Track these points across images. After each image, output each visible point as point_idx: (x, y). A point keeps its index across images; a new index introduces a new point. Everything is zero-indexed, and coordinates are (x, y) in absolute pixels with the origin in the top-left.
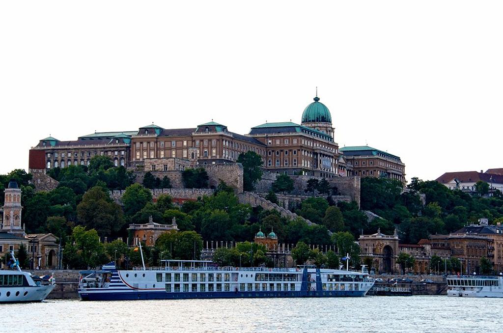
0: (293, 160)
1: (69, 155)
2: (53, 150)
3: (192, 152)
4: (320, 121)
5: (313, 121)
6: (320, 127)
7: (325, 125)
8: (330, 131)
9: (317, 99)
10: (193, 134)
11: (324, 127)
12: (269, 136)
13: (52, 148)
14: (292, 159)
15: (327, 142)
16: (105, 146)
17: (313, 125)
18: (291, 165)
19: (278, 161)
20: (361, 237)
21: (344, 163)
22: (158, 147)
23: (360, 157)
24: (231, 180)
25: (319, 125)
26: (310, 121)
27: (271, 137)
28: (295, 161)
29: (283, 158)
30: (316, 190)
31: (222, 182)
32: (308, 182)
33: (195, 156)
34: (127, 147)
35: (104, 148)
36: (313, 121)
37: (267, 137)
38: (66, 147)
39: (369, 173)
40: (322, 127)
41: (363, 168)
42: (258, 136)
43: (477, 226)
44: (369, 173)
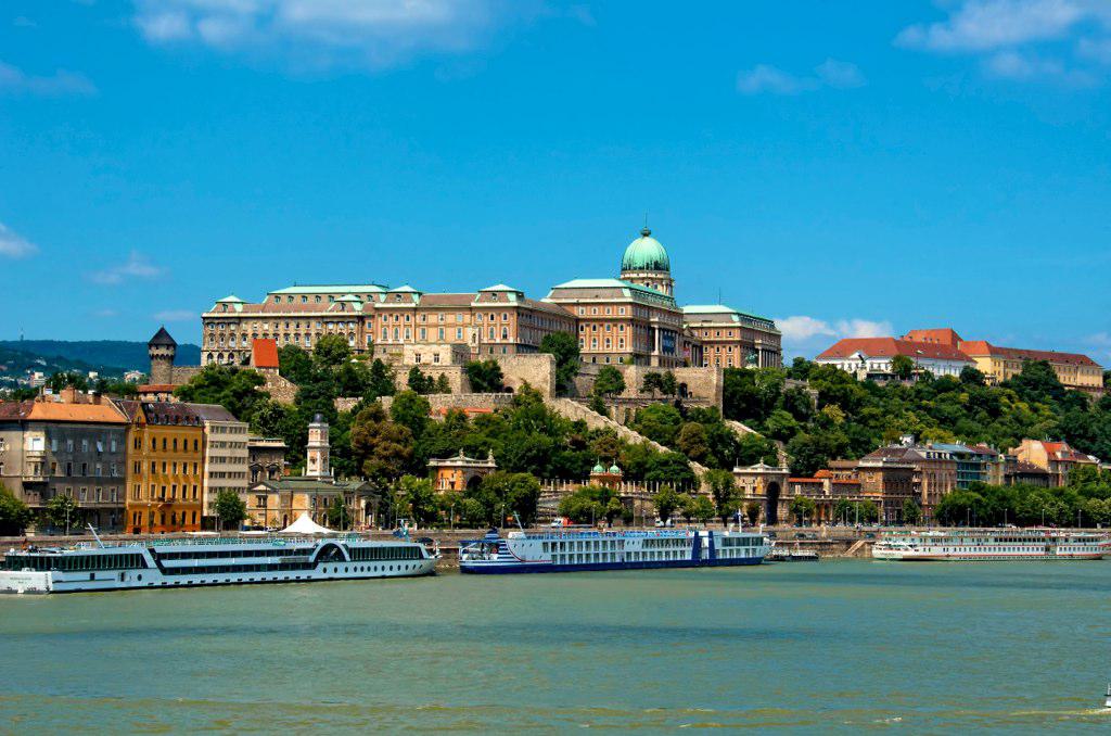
1: (266, 327)
2: (240, 318)
5: (640, 268)
10: (473, 304)
13: (236, 315)
16: (324, 314)
17: (641, 275)
18: (615, 348)
19: (595, 340)
20: (736, 470)
23: (712, 325)
24: (537, 379)
25: (650, 275)
26: (635, 269)
28: (622, 341)
30: (657, 389)
31: (525, 383)
32: (646, 377)
33: (477, 338)
34: (358, 317)
35: (323, 317)
37: (578, 304)
38: (261, 314)
43: (898, 446)
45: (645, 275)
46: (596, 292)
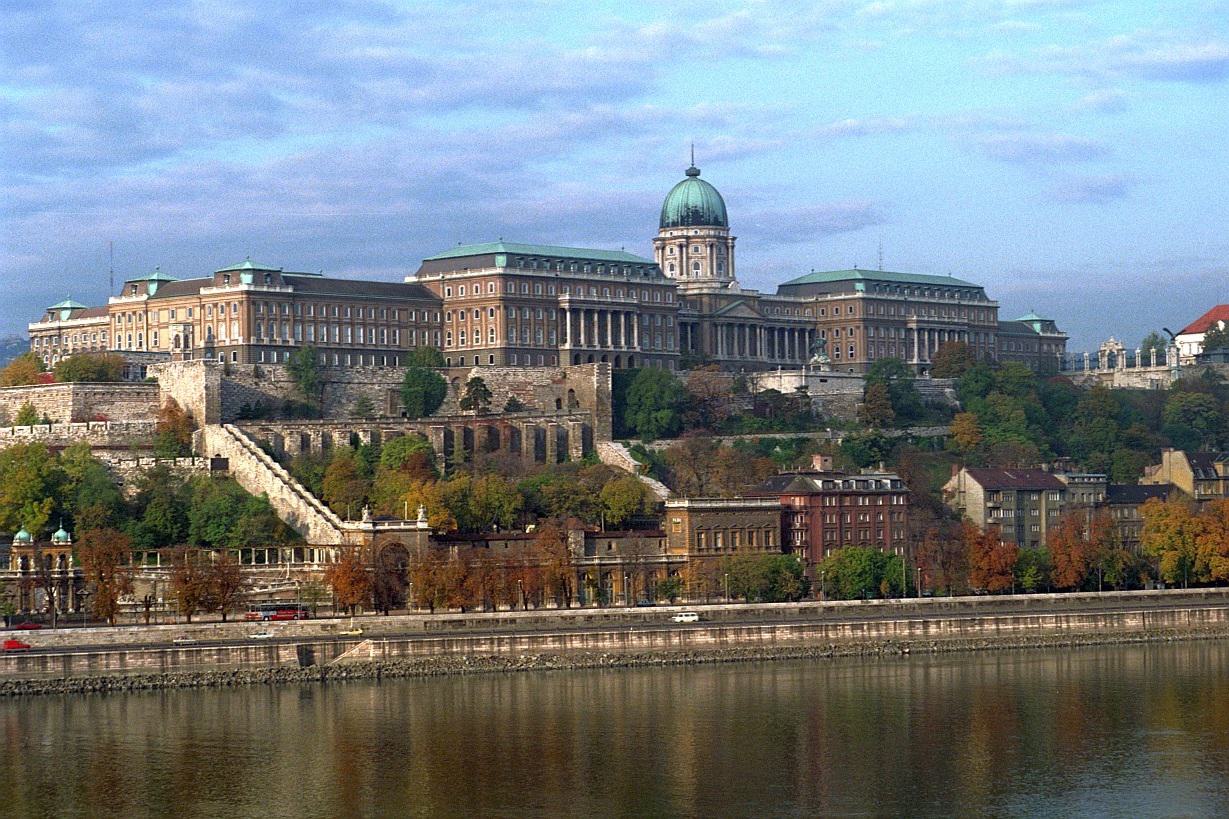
0: (489, 330)
3: (175, 333)
4: (688, 225)
6: (688, 238)
7: (700, 233)
8: (711, 246)
9: (693, 173)
11: (699, 237)
12: (448, 277)
14: (486, 329)
15: (624, 280)
17: (675, 233)
21: (755, 315)
22: (150, 322)
25: (685, 233)
27: (450, 280)
29: (472, 328)
36: (675, 224)
37: (443, 281)
39: (846, 334)
40: (694, 237)
41: (836, 322)
42: (428, 278)
44: (846, 334)
45: (679, 233)
46: (464, 262)
